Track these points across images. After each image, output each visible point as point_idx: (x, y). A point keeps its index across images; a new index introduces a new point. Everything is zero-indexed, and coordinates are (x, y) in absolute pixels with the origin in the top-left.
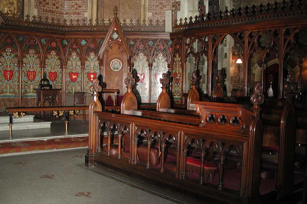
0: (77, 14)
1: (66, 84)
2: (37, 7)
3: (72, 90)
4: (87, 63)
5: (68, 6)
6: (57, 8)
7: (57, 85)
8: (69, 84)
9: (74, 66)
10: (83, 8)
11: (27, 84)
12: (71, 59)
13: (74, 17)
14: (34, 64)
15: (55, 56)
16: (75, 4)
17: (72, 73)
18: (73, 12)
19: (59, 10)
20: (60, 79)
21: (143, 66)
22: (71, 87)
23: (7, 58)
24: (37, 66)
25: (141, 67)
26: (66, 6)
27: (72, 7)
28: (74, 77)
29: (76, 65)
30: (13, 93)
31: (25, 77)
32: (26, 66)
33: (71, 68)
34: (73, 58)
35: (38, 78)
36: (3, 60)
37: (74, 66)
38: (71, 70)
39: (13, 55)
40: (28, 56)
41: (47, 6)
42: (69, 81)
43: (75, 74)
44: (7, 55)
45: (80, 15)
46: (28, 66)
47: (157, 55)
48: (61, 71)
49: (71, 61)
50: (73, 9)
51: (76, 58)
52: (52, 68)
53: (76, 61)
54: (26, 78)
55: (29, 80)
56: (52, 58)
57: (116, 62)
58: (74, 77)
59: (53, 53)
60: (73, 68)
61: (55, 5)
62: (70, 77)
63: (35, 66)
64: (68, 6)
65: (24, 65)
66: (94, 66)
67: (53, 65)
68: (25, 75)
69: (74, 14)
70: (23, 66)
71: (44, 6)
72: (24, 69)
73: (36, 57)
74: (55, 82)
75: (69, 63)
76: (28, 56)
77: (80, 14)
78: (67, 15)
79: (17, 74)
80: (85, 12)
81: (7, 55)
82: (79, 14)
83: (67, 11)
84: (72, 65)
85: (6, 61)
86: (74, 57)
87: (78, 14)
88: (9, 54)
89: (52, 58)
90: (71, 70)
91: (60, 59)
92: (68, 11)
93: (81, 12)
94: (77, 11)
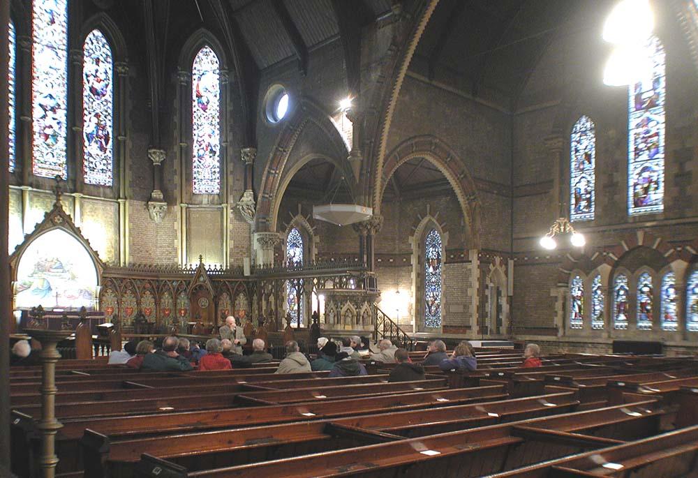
6: (150, 254)
10: (173, 254)
13: (165, 262)
39: (113, 295)
47: (238, 295)
76: (126, 295)
88: (109, 293)
91: (154, 298)
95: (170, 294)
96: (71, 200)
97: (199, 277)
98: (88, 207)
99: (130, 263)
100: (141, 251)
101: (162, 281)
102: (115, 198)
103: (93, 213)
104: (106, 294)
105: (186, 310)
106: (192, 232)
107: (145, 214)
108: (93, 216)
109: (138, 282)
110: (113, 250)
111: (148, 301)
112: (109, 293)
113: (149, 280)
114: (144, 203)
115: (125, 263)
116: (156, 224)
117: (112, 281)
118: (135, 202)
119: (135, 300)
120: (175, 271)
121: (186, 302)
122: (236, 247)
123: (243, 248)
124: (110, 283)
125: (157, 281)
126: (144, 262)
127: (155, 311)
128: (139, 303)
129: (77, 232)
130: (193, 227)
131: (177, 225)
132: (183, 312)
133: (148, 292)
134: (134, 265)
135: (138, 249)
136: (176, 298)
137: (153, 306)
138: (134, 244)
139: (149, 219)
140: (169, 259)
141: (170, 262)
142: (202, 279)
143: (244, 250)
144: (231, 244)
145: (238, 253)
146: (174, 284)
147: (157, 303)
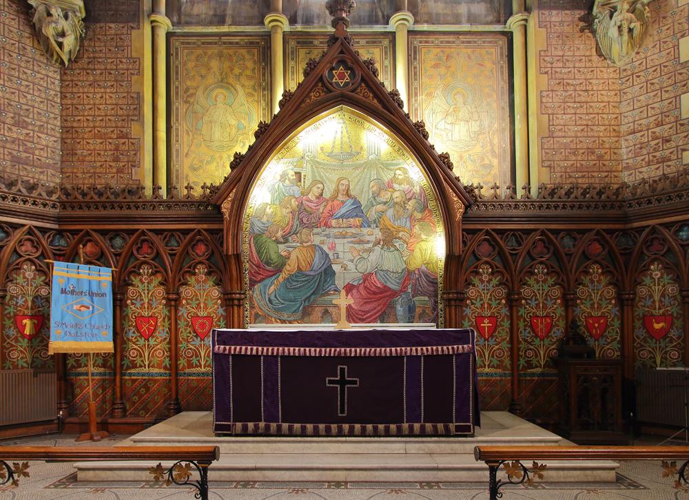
1: (635, 344)
2: (547, 163)
3: (653, 360)
5: (630, 149)
8: (642, 346)
9: (657, 298)
11: (532, 347)
14: (546, 300)
15: (600, 275)
16: (650, 139)
17: (652, 315)
18: (647, 159)
19: (607, 163)
20: (617, 332)
22: (650, 352)
23: (481, 287)
24: (555, 303)
26: (624, 151)
27: (641, 148)
28: (657, 326)
29: (663, 295)
30: (498, 367)
31: (525, 330)
32: (527, 304)
33: (649, 303)
34: (652, 278)
35: (558, 332)
36: (472, 293)
37: (657, 298)
38: (647, 309)
40: (531, 281)
41: (574, 158)
42: (642, 337)
44: (482, 282)
46: (533, 304)
49: (646, 285)
50: (644, 151)
51: (661, 277)
52: (592, 305)
53: (662, 284)
54: (529, 333)
55: (536, 336)
56: (592, 281)
58: (657, 326)
59: (596, 270)
61: (593, 153)
62: (645, 327)
63: (549, 304)
64: (630, 149)
65: (523, 301)
67: (596, 299)
68: (525, 326)
69: (649, 164)
70: (521, 305)
72: (522, 311)
73: (551, 281)
74: (602, 341)
75: (642, 291)
76: (531, 281)
77: (670, 160)
78: (626, 173)
79: (507, 324)
81: (482, 282)
82: (664, 160)
83: (628, 161)
84: (651, 296)
85: (481, 296)
86: (656, 275)
88: (485, 277)
89: (592, 281)
90: (647, 309)
92: (631, 161)
94: (658, 154)
96: (386, 42)
98: (429, 55)
99: (542, 187)
102: (498, 22)
103: (442, 70)
104: (476, 281)
107: (583, 46)
108: (442, 77)
109: (567, 241)
110: (495, 162)
111: (597, 297)
112: (485, 277)
113: (598, 233)
114: (579, 13)
115: (527, 188)
117: (493, 243)
118: (555, 16)
119: (557, 292)
124: (486, 248)
125: (625, 232)
127: (617, 323)
128: (569, 302)
129: (385, 109)
133: (596, 269)
134: (553, 193)
137: (611, 309)
138: (551, 135)
139: (595, 58)
147: (625, 301)
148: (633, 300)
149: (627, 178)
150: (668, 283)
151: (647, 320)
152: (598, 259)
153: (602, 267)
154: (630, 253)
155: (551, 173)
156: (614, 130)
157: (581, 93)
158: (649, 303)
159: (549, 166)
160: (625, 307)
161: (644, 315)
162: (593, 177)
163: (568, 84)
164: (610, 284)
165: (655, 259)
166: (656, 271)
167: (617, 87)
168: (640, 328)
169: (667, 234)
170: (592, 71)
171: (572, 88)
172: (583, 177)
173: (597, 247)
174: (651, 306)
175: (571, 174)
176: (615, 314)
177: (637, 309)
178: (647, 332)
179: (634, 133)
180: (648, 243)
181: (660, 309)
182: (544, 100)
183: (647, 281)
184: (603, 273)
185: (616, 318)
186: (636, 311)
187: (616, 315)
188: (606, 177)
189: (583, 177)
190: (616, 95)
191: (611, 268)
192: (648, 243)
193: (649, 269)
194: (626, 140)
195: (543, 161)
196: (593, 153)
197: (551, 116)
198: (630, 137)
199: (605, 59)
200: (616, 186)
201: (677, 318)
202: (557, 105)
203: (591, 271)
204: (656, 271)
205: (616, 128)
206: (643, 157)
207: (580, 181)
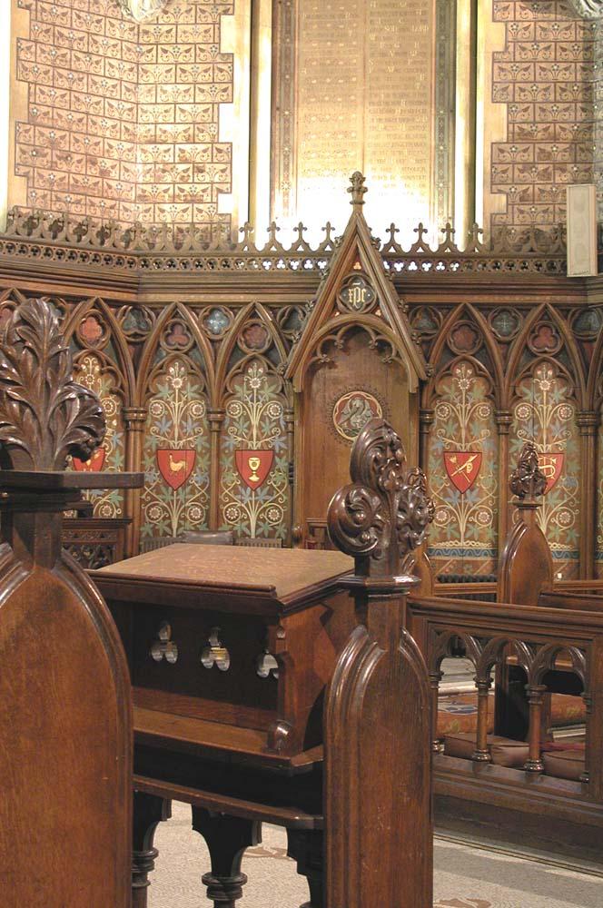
0: (186, 202)
1: (143, 497)
2: (23, 170)
4: (236, 408)
5: (148, 167)
6: (104, 173)
7: (105, 503)
8: (153, 499)
9: (176, 420)
10: (213, 174)
12: (164, 391)
13: (173, 214)
16: (177, 160)
17: (169, 449)
18: (171, 192)
19: (113, 184)
21: (471, 420)
25: (464, 422)
27: (164, 171)
28: (176, 467)
29: (184, 418)
33: (165, 429)
34: (171, 387)
37: (176, 420)
38: (163, 439)
41: (65, 168)
42: (154, 485)
43: (180, 454)
45: (201, 206)
48: (120, 443)
49: (161, 398)
50: (168, 178)
51: (183, 388)
53: (184, 399)
57: (357, 403)
58: (176, 467)
59: (91, 367)
60: (172, 427)
61: (94, 163)
62: (158, 468)
64: (148, 167)
66: (262, 419)
69: (174, 199)
71: (51, 168)
75: (157, 406)
78: (142, 207)
80: (220, 191)
83: (144, 187)
84: (169, 418)
86: (177, 383)
87: (193, 202)
90: (163, 439)
92: (148, 188)
93: (204, 191)
94: (186, 187)
95: (197, 373)
97: (346, 285)
100: (66, 157)
101: (157, 308)
105: (269, 456)
106: (302, 73)
116: (137, 30)
120: (217, 256)
121: (274, 409)
122: (519, 136)
123: (555, 139)
125: (136, 307)
126: (78, 212)
130: (307, 47)
131: (233, 33)
132: (254, 463)
135: (53, 144)
136: (227, 394)
138: (32, 120)
140: (194, 199)
141: (198, 216)
142: (358, 295)
143: (559, 151)
144: (493, 121)
145: (527, 167)
146: (215, 323)
148: (143, 421)
149: (132, 214)
150: (193, 399)
151: (161, 455)
152: (96, 347)
153: (101, 363)
154: (143, 343)
155: (28, 187)
156: (127, 129)
157: (80, 55)
158: (165, 429)
159: (26, 175)
160: (132, 434)
161: (158, 449)
162: (93, 204)
163: (61, 35)
164: (112, 392)
165: (177, 357)
166: (177, 376)
167: (133, 57)
168: (151, 468)
169: (193, 319)
170: (98, 22)
171: (67, 44)
172: (78, 202)
173: (93, 330)
174: (168, 433)
175: (59, 195)
176: (117, 444)
177: (227, 438)
178: (162, 475)
179: (155, 142)
180: (169, 330)
181: (180, 439)
182: (22, 55)
183: (164, 391)
184: (101, 373)
185: (117, 452)
186: (147, 441)
187: (117, 444)
188: (112, 207)
189: (78, 202)
190: (131, 70)
191: (115, 367)
192: (169, 330)
193: (167, 373)
194: (144, 151)
195: (16, 165)
196: (94, 163)
197: (32, 86)
198: (150, 147)
199: (118, 4)
200: (125, 226)
201: (202, 455)
202: (43, 68)
203: (84, 367)
204: (177, 376)
205: (130, 126)
206: (165, 187)
207: (73, 209)
